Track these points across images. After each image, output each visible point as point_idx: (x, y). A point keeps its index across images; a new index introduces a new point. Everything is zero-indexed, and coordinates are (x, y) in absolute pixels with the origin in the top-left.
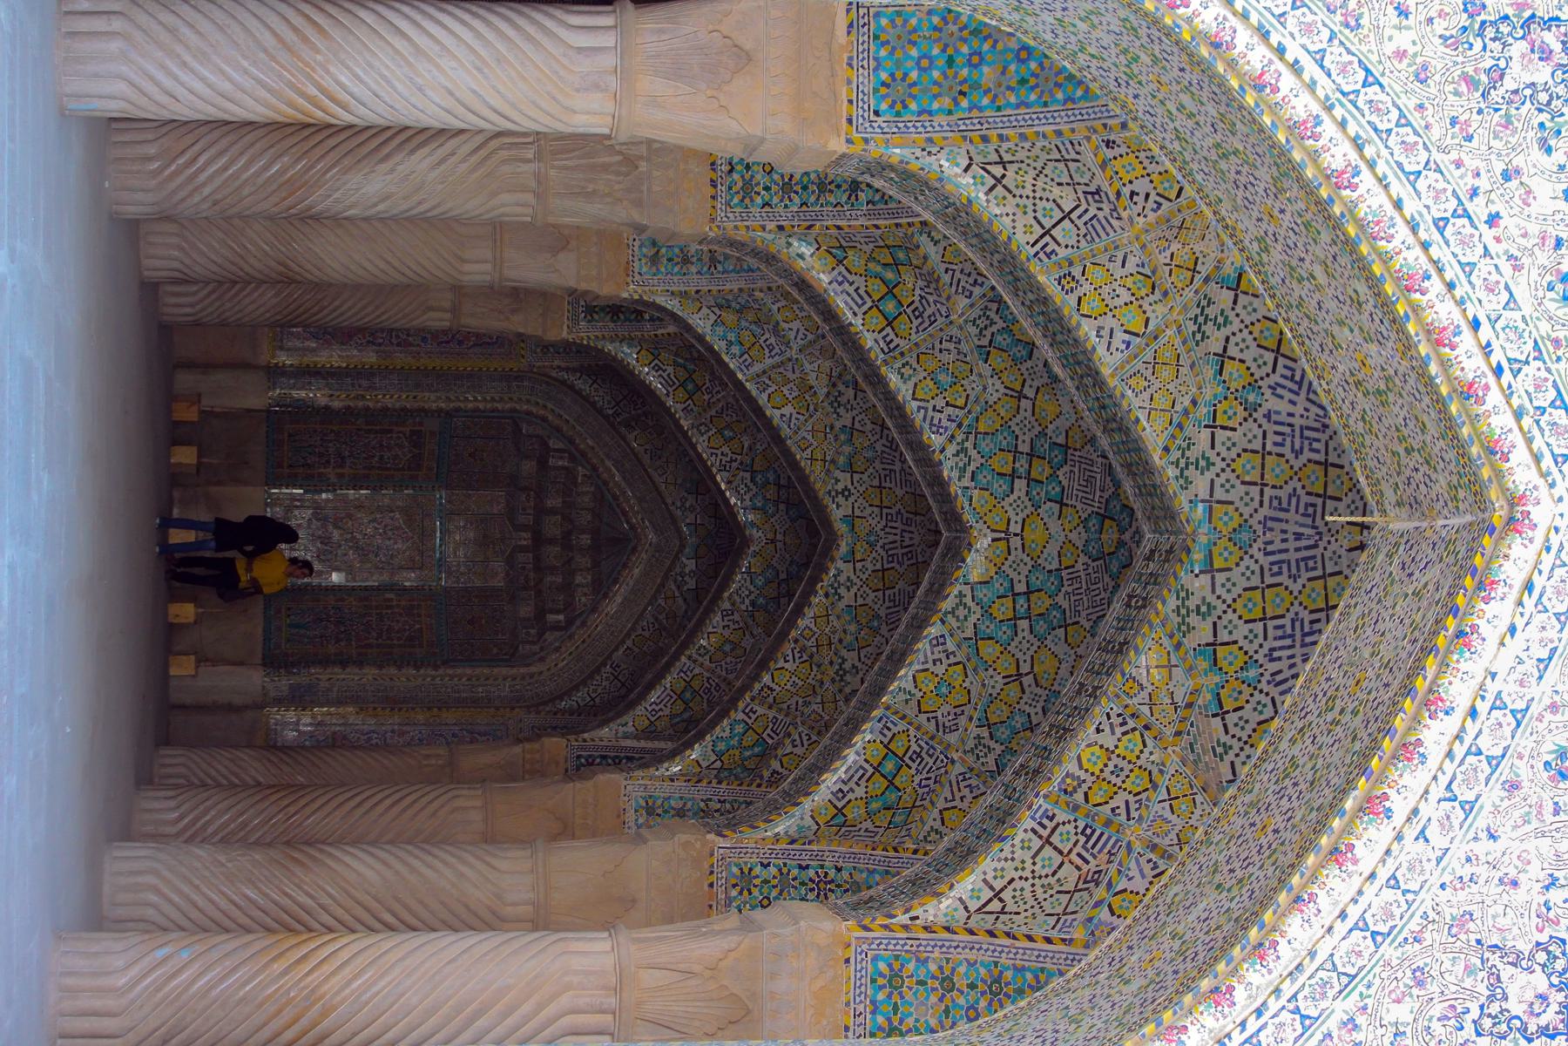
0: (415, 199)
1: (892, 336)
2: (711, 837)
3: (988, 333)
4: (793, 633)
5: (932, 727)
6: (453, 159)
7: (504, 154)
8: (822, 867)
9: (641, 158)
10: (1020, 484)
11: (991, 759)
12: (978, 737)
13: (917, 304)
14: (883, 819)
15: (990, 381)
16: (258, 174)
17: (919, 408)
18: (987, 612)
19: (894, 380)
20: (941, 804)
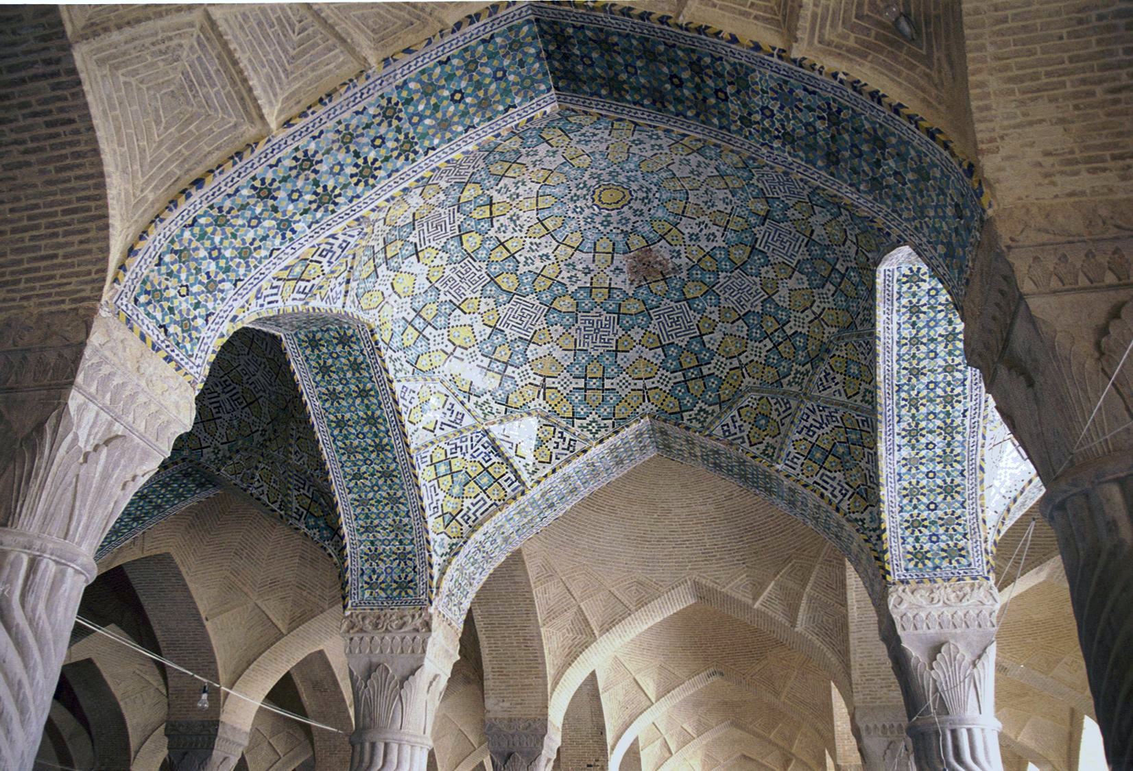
14: (473, 489)
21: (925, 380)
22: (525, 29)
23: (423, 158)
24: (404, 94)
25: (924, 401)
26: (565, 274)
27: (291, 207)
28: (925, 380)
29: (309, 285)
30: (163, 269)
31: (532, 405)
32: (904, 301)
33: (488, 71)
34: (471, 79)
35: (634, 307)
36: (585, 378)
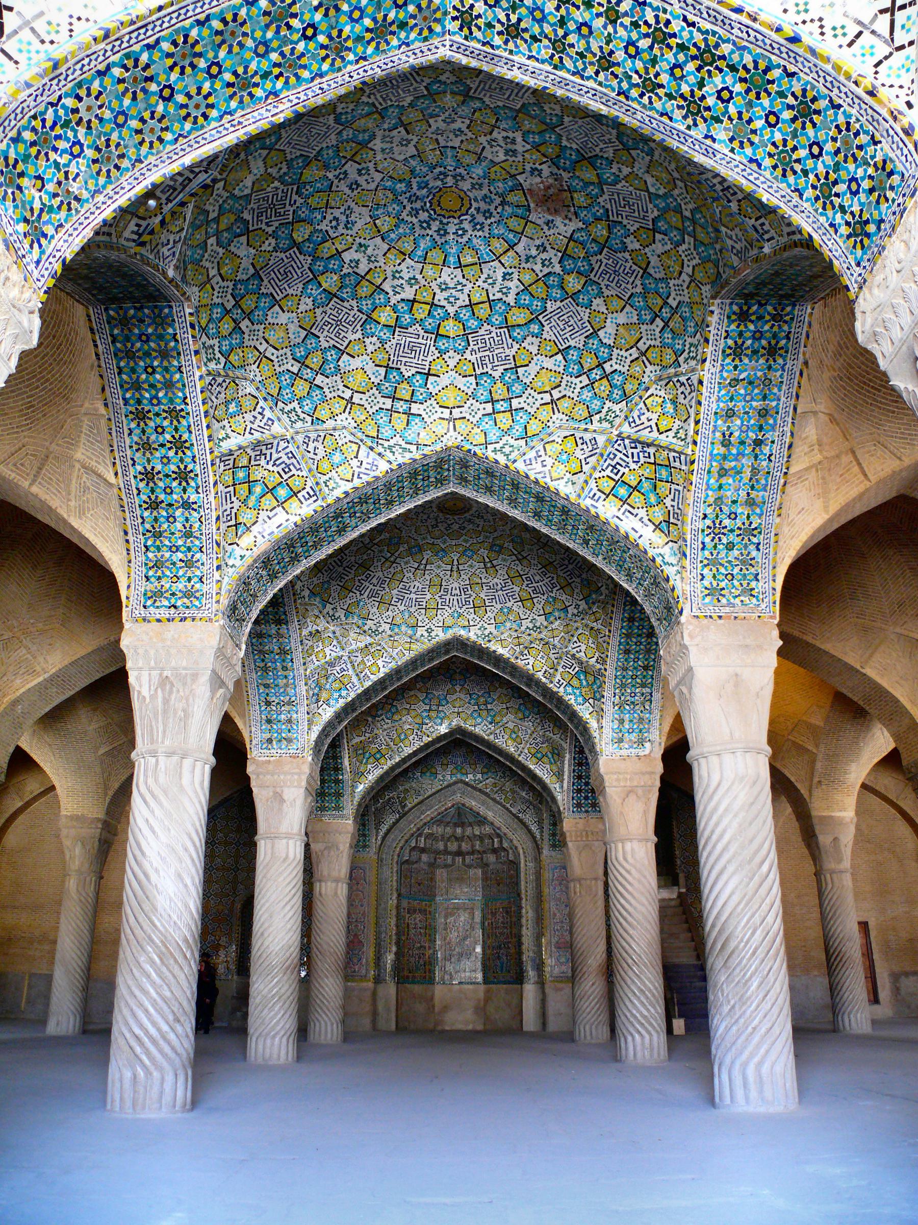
0: (182, 852)
1: (304, 493)
2: (683, 619)
3: (302, 416)
4: (512, 660)
5: (592, 460)
6: (151, 820)
7: (150, 781)
8: (703, 531)
9: (161, 675)
10: (415, 408)
11: (616, 408)
12: (600, 421)
13: (279, 469)
14: (663, 488)
15: (339, 422)
16: (153, 983)
17: (359, 477)
18: (507, 432)
19: (338, 493)
20: (655, 434)
21: (620, 55)
22: (112, 313)
23: (189, 407)
24: (132, 402)
25: (652, 72)
26: (538, 268)
27: (175, 496)
28: (620, 55)
29: (308, 489)
30: (153, 580)
31: (646, 379)
32: (498, 41)
33: (138, 345)
34: (140, 358)
35: (600, 231)
36: (657, 316)
